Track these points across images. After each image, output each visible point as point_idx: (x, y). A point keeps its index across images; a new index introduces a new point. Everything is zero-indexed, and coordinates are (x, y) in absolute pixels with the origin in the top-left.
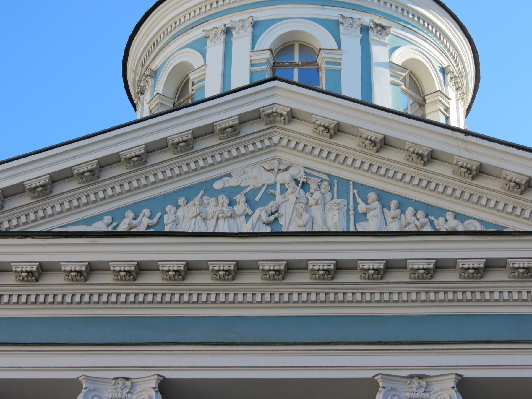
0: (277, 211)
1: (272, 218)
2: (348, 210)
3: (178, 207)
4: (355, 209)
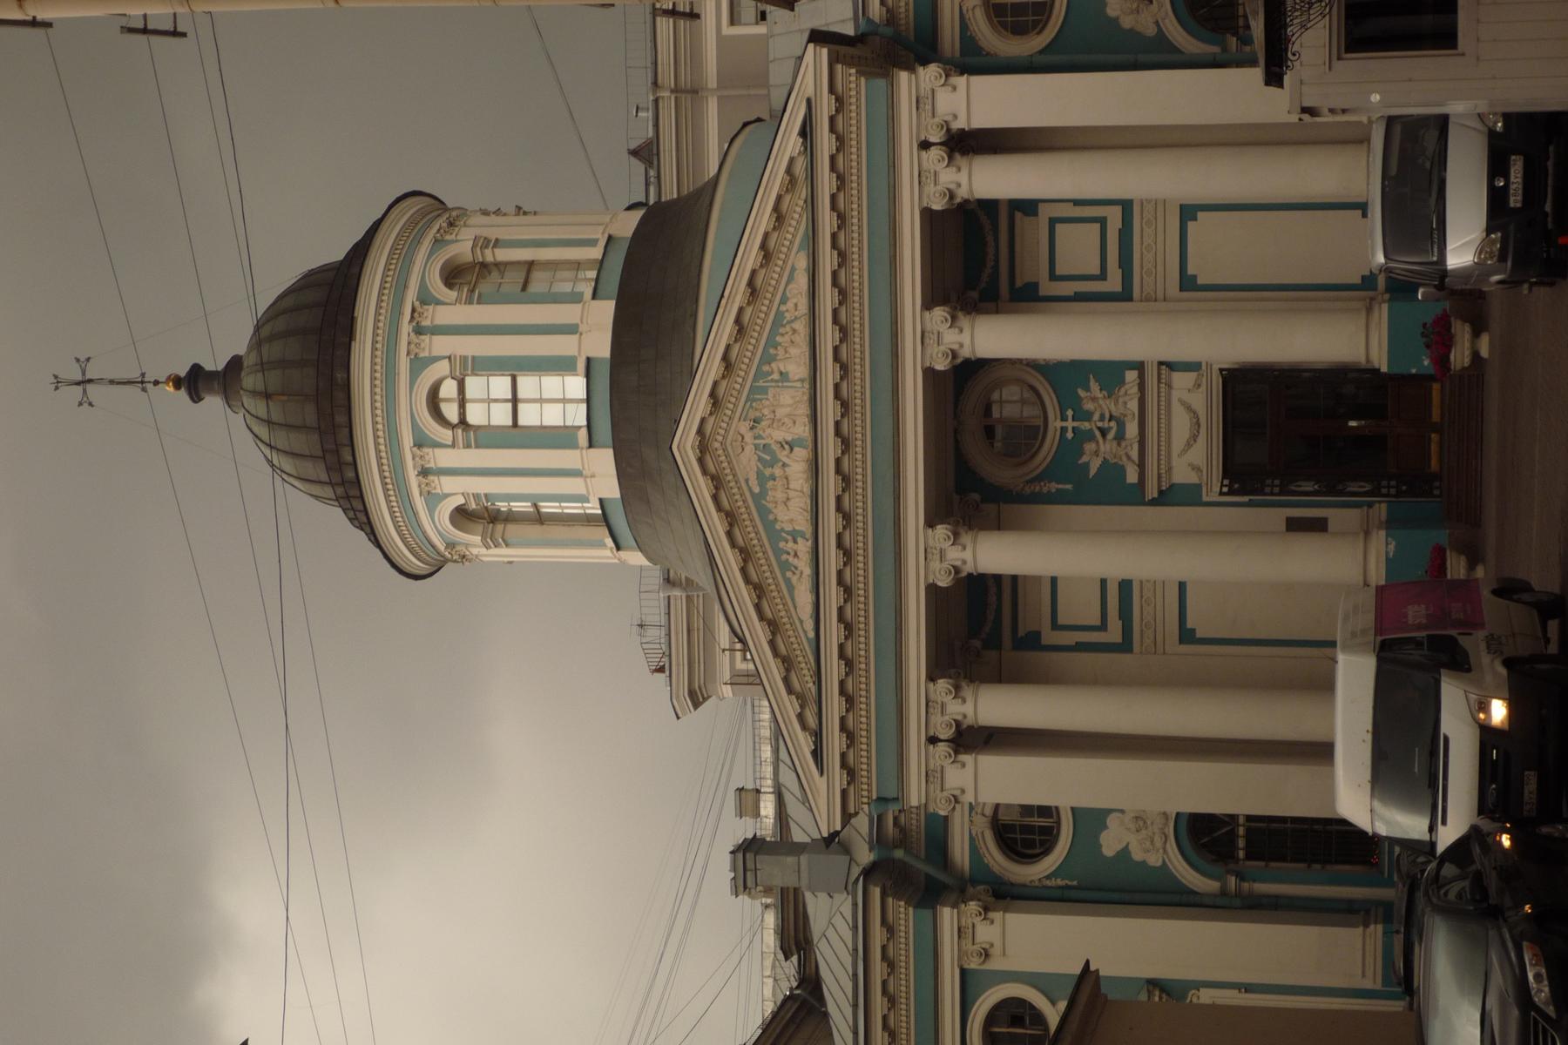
0: (780, 443)
1: (787, 447)
2: (778, 387)
4: (777, 381)
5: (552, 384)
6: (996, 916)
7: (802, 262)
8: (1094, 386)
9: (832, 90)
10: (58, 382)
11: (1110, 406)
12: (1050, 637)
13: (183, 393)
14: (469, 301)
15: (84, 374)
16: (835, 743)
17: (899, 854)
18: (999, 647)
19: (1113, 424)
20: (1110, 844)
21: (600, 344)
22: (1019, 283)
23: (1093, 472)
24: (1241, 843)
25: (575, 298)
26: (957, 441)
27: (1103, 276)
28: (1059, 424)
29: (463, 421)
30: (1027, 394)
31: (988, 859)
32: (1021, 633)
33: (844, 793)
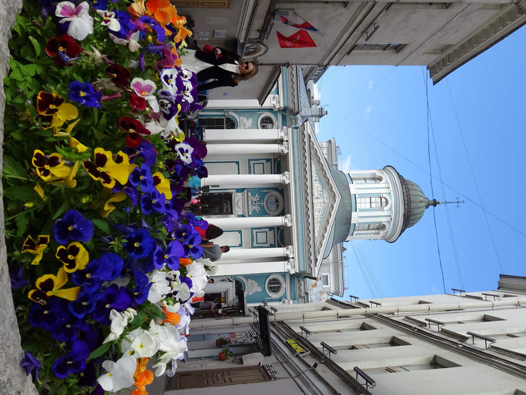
3: (320, 183)
5: (363, 206)
6: (272, 106)
7: (316, 234)
8: (257, 211)
9: (312, 268)
10: (463, 202)
11: (255, 207)
12: (264, 161)
13: (437, 201)
14: (380, 222)
15: (458, 204)
16: (306, 140)
17: (292, 117)
18: (274, 159)
19: (254, 204)
20: (250, 121)
21: (354, 214)
22: (273, 230)
23: (257, 194)
24: (225, 122)
25: (358, 223)
26: (284, 199)
27: (257, 232)
28: (264, 203)
29: (381, 198)
30: (270, 209)
31: (274, 116)
32: (270, 162)
33: (304, 130)
